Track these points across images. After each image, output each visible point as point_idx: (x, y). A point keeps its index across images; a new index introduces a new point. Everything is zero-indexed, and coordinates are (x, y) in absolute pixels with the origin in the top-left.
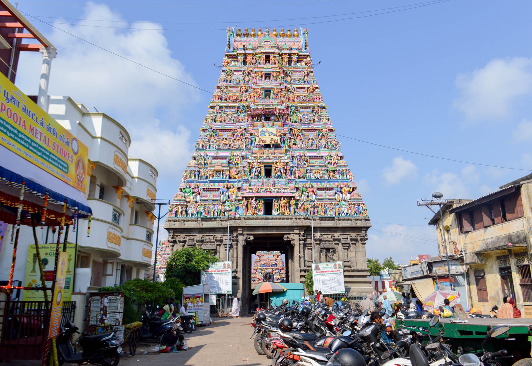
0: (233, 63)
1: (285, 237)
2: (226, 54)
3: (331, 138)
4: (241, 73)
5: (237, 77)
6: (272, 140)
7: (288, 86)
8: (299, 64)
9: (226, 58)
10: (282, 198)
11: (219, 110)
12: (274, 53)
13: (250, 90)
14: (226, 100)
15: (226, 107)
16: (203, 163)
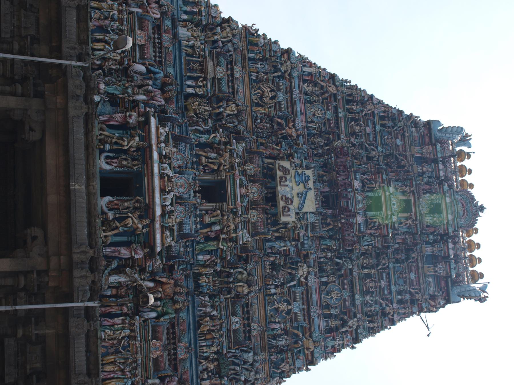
1: (37, 232)
3: (293, 361)
6: (288, 201)
8: (431, 280)
10: (148, 222)
16: (216, 38)
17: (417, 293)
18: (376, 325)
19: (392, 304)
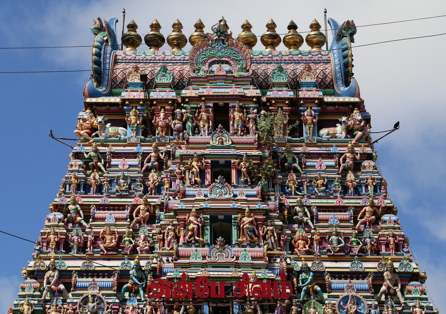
0: (111, 129)
2: (88, 100)
4: (135, 162)
5: (120, 174)
7: (289, 202)
8: (324, 131)
9: (86, 114)
11: (57, 283)
12: (242, 98)
13: (162, 215)
14: (82, 248)
15: (82, 274)
17: (344, 160)
18: (391, 239)
19: (362, 207)
